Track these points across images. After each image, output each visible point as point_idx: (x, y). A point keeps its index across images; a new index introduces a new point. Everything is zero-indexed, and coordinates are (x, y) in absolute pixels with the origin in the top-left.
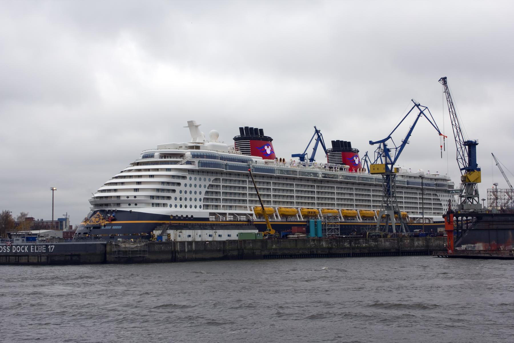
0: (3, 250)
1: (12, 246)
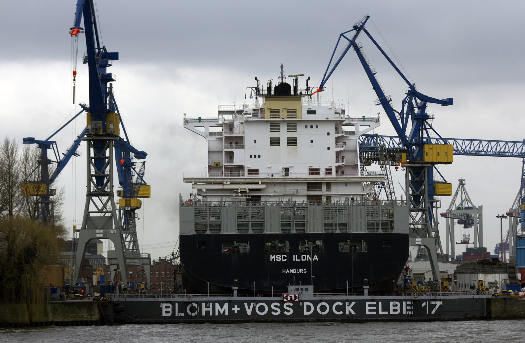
0: (270, 310)
1: (303, 301)
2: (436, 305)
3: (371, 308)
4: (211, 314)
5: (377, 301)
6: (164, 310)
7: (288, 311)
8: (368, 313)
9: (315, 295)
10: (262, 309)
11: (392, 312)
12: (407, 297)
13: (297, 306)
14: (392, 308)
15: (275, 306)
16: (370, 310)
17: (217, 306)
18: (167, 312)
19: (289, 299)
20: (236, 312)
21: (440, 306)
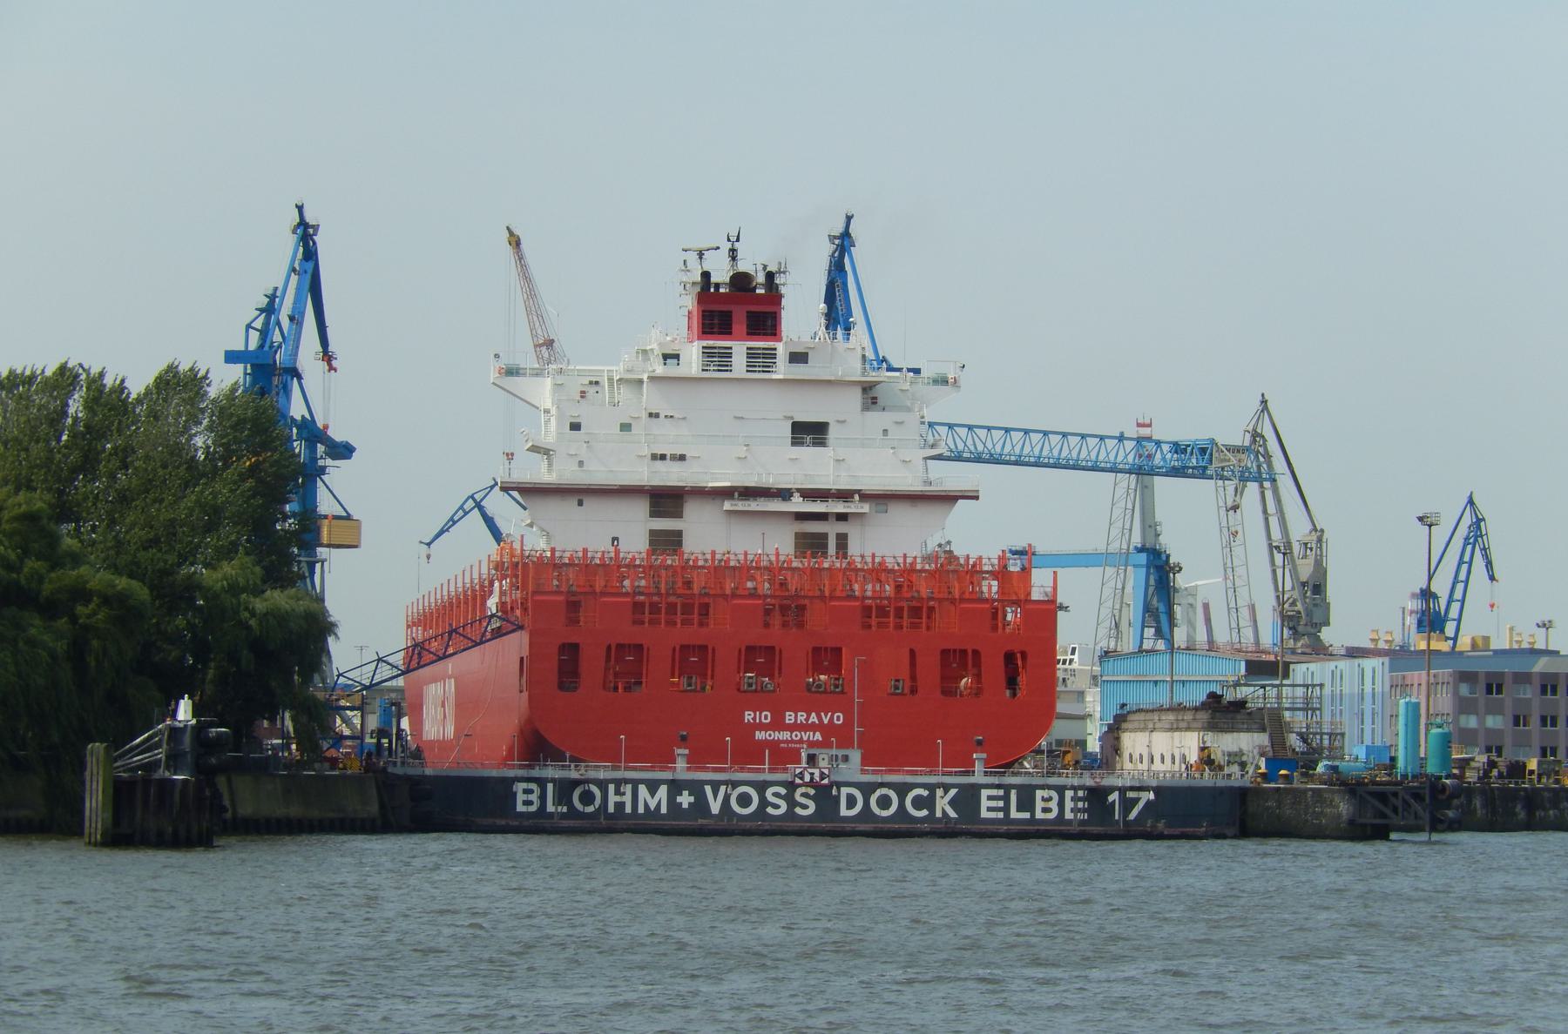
0: (764, 803)
1: (839, 785)
2: (1138, 800)
3: (993, 804)
4: (628, 810)
5: (1007, 788)
6: (521, 797)
7: (805, 807)
8: (984, 814)
9: (863, 772)
10: (744, 800)
11: (1039, 815)
12: (1076, 782)
13: (825, 795)
14: (1039, 804)
15: (776, 795)
16: (989, 809)
17: (643, 789)
18: (528, 803)
19: (807, 778)
20: (685, 806)
21: (1148, 802)
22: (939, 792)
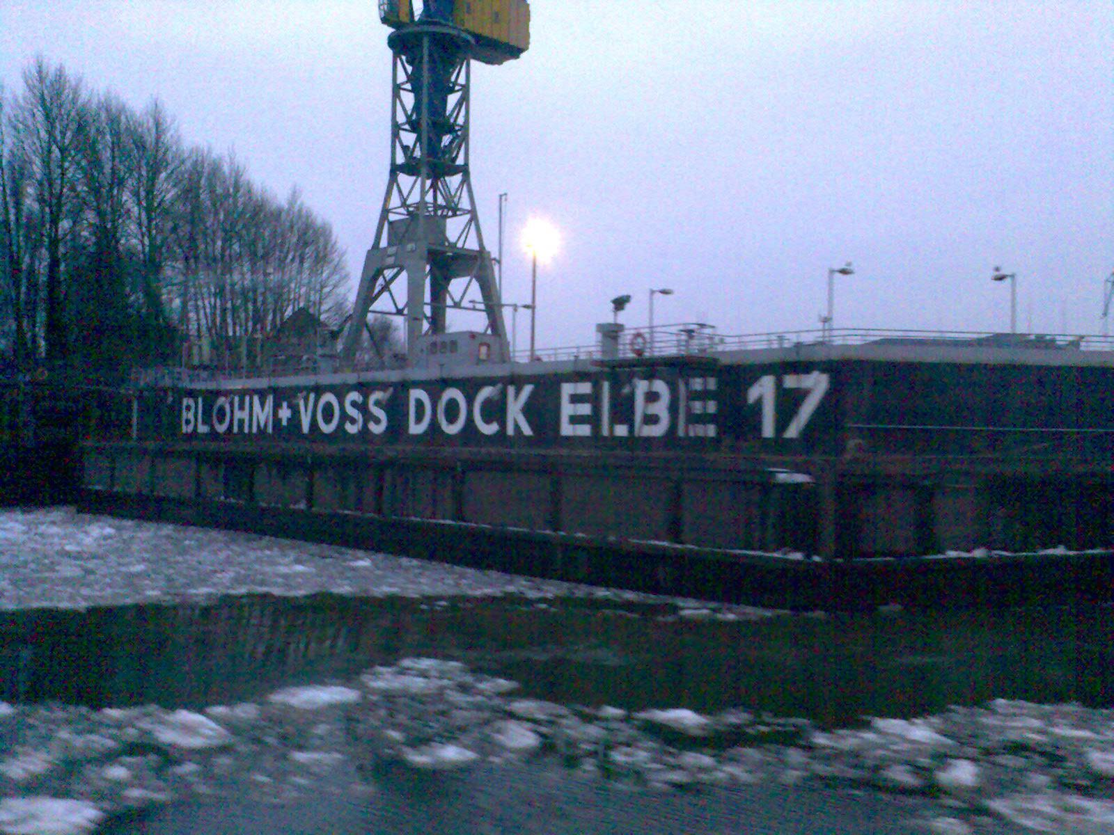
0: (345, 417)
1: (403, 387)
8: (567, 429)
10: (328, 414)
16: (575, 420)
17: (256, 399)
20: (284, 423)
22: (511, 390)
